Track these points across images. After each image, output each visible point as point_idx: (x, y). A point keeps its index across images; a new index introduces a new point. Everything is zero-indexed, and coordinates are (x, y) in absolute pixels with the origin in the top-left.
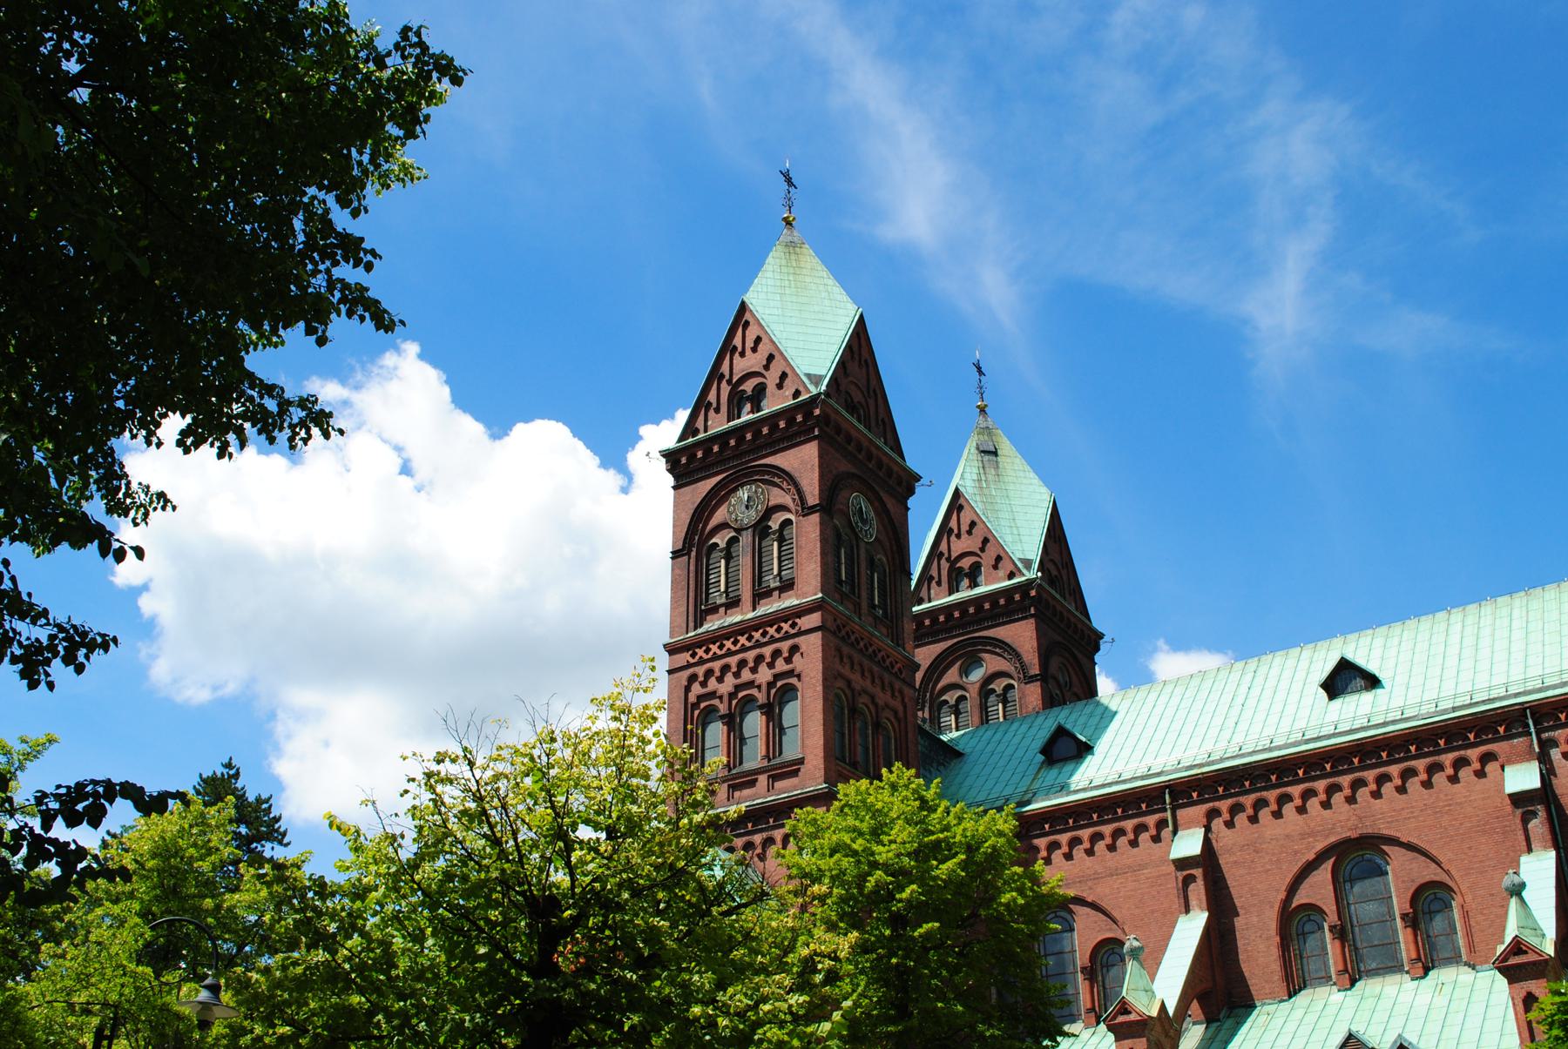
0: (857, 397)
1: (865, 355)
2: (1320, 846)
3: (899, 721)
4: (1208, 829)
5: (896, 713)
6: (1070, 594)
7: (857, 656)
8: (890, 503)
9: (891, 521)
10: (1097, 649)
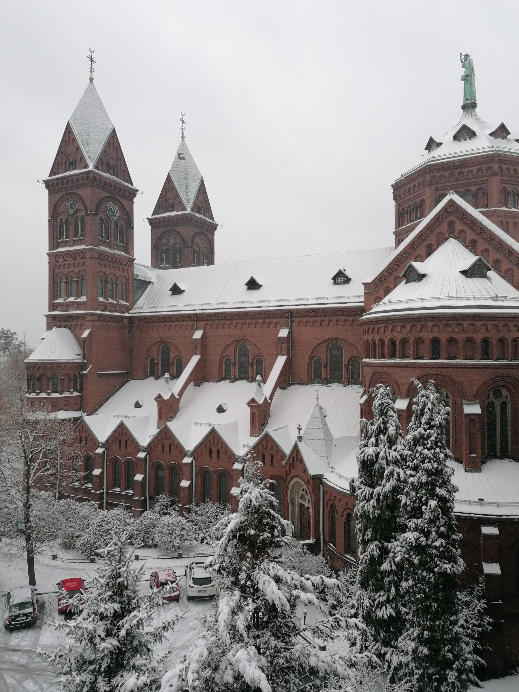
0: (112, 163)
1: (116, 145)
2: (232, 340)
4: (205, 330)
5: (125, 277)
7: (107, 263)
8: (125, 203)
10: (216, 229)
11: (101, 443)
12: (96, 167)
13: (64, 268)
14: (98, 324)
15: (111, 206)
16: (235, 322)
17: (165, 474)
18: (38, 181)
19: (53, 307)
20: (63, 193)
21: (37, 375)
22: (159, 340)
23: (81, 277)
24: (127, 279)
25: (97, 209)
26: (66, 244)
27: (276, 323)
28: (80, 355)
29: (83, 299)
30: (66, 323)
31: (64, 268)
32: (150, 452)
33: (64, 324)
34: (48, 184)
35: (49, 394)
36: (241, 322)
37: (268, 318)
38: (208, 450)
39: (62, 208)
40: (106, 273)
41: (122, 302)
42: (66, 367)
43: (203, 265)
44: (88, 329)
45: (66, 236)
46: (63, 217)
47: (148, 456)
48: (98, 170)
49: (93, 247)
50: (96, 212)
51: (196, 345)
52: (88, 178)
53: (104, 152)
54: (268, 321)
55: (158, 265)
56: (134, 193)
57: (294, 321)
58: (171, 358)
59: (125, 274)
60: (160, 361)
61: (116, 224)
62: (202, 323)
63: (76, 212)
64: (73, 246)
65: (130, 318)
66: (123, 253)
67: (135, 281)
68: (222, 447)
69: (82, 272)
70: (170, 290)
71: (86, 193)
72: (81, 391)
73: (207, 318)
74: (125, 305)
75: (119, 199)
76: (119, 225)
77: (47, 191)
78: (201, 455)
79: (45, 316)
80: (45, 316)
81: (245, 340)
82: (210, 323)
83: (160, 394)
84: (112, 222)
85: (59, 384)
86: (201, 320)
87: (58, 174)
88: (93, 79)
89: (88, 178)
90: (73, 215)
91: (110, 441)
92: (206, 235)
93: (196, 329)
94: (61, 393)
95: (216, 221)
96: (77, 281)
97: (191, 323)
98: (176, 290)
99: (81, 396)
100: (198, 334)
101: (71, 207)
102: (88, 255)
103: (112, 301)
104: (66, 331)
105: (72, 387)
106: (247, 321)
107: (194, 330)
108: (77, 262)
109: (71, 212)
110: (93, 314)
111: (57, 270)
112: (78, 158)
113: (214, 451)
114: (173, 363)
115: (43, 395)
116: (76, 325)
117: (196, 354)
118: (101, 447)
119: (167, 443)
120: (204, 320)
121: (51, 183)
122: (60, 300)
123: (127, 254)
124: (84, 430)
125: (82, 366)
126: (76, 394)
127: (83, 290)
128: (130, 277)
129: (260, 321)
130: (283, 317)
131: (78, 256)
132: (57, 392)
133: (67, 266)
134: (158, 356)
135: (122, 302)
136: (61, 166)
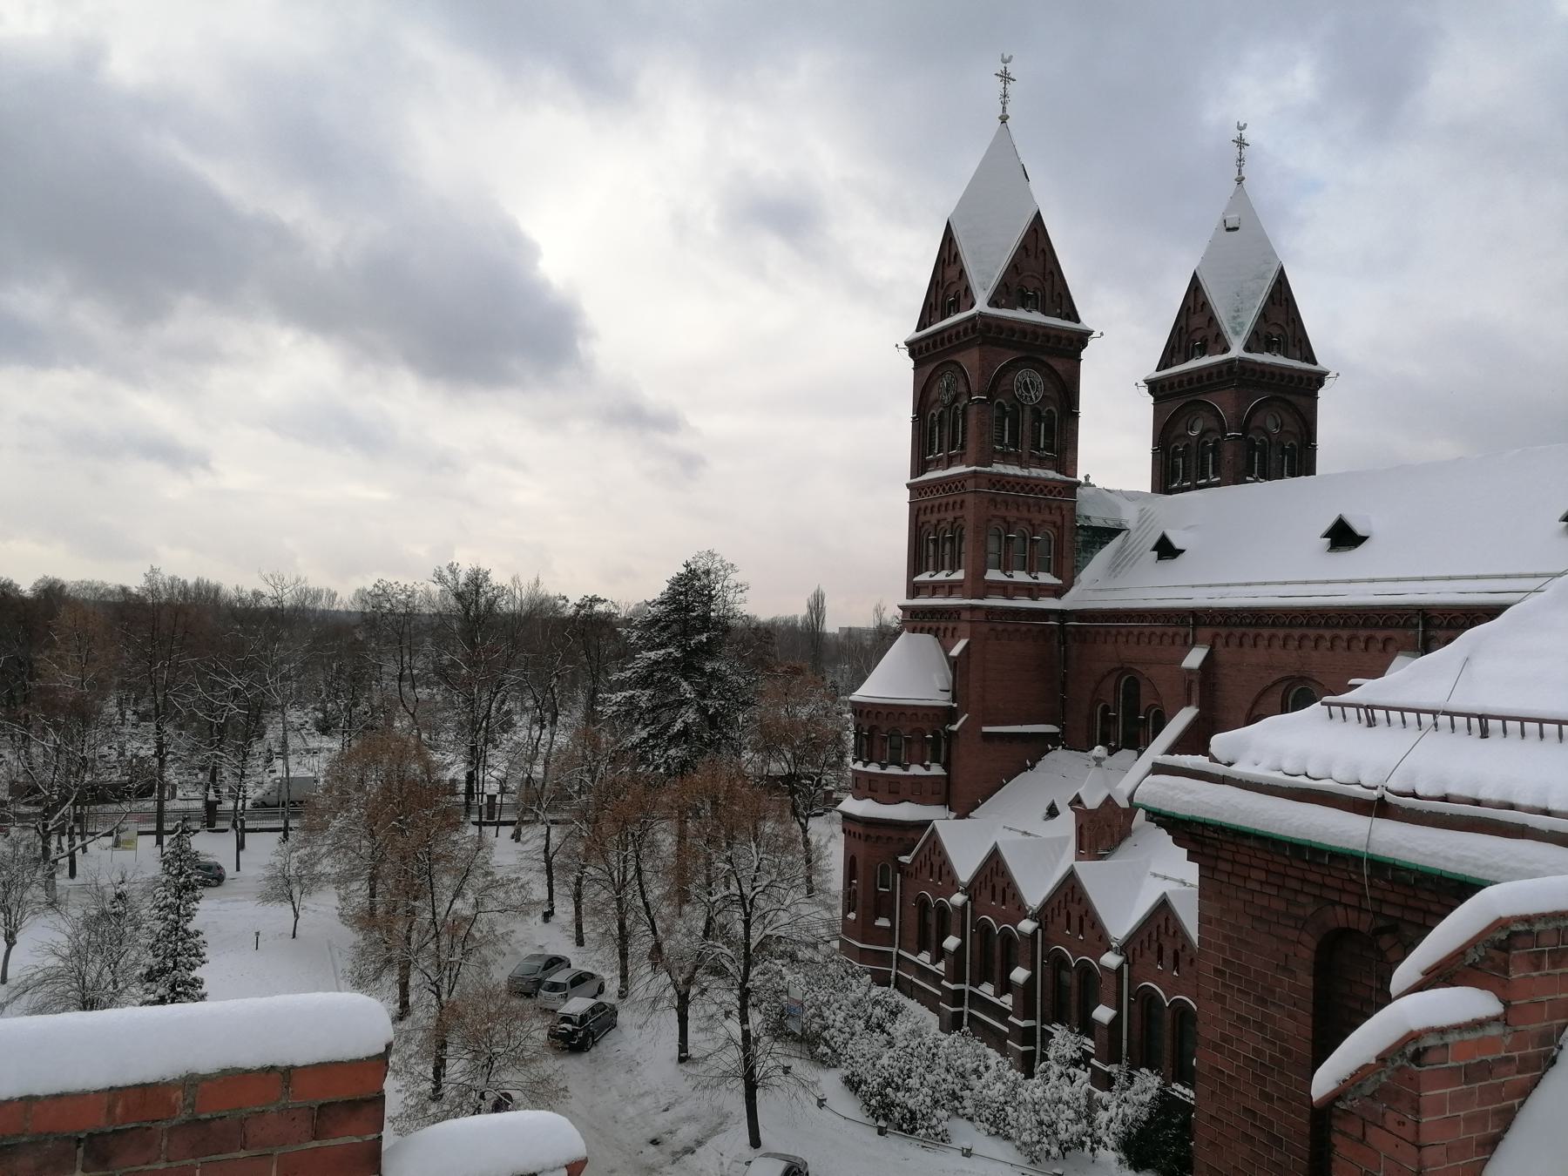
2: (1276, 677)
3: (1058, 528)
5: (1054, 524)
6: (1294, 346)
8: (1059, 365)
9: (1059, 376)
11: (962, 884)
12: (993, 303)
13: (932, 512)
14: (985, 628)
15: (1024, 375)
16: (1281, 633)
17: (1070, 979)
18: (897, 346)
19: (914, 590)
20: (933, 366)
21: (867, 728)
22: (1117, 665)
23: (959, 530)
24: (1059, 528)
25: (992, 392)
26: (938, 464)
27: (1386, 641)
28: (948, 691)
29: (959, 575)
30: (931, 624)
31: (932, 512)
32: (1044, 923)
33: (927, 625)
34: (914, 348)
35: (883, 767)
36: (1297, 633)
37: (1364, 626)
38: (1155, 947)
39: (934, 394)
40: (1008, 519)
41: (1046, 578)
42: (916, 714)
43: (1281, 477)
44: (965, 637)
45: (938, 449)
46: (935, 411)
47: (1039, 930)
48: (998, 307)
49: (979, 469)
50: (989, 395)
51: (1191, 682)
52: (974, 327)
53: (1014, 267)
54: (1363, 634)
55: (1166, 487)
56: (1081, 339)
57: (1433, 637)
58: (1142, 709)
59: (1059, 521)
60: (1121, 713)
61: (1036, 412)
62: (1206, 632)
63: (955, 399)
64: (948, 467)
65: (1062, 614)
66: (1052, 474)
67: (1081, 531)
68: (1183, 946)
69: (960, 521)
70: (1154, 550)
71: (970, 360)
72: (946, 766)
73: (1218, 620)
74: (1053, 585)
75: (1045, 358)
76: (1044, 414)
77: (911, 363)
78: (1141, 955)
79: (901, 607)
80: (901, 607)
81: (1305, 677)
82: (1224, 632)
83: (1078, 795)
84: (1028, 411)
85: (903, 750)
86: (1205, 624)
87: (930, 325)
88: (1008, 117)
89: (974, 327)
90: (951, 405)
91: (977, 884)
92: (1289, 403)
93: (1194, 644)
94: (906, 768)
95: (1323, 362)
96: (952, 539)
97: (1182, 631)
98: (1166, 549)
99: (948, 778)
100: (1194, 658)
101: (948, 391)
102: (970, 485)
103: (1020, 576)
104: (927, 640)
105: (929, 757)
106: (1312, 633)
107: (1187, 647)
108: (951, 501)
109: (946, 399)
110: (973, 608)
111: (922, 518)
112: (962, 293)
113: (1168, 952)
114: (1146, 721)
115: (874, 768)
116: (946, 629)
117: (1189, 704)
118: (962, 892)
119: (1076, 911)
120: (1210, 625)
121: (916, 347)
122: (924, 577)
123: (1061, 473)
124: (937, 853)
125: (949, 714)
126: (937, 770)
127: (963, 556)
128: (1067, 524)
129: (1345, 634)
130: (1405, 626)
131: (953, 487)
132: (900, 766)
133: (929, 511)
134: (1116, 699)
135: (1046, 578)
136: (936, 309)
